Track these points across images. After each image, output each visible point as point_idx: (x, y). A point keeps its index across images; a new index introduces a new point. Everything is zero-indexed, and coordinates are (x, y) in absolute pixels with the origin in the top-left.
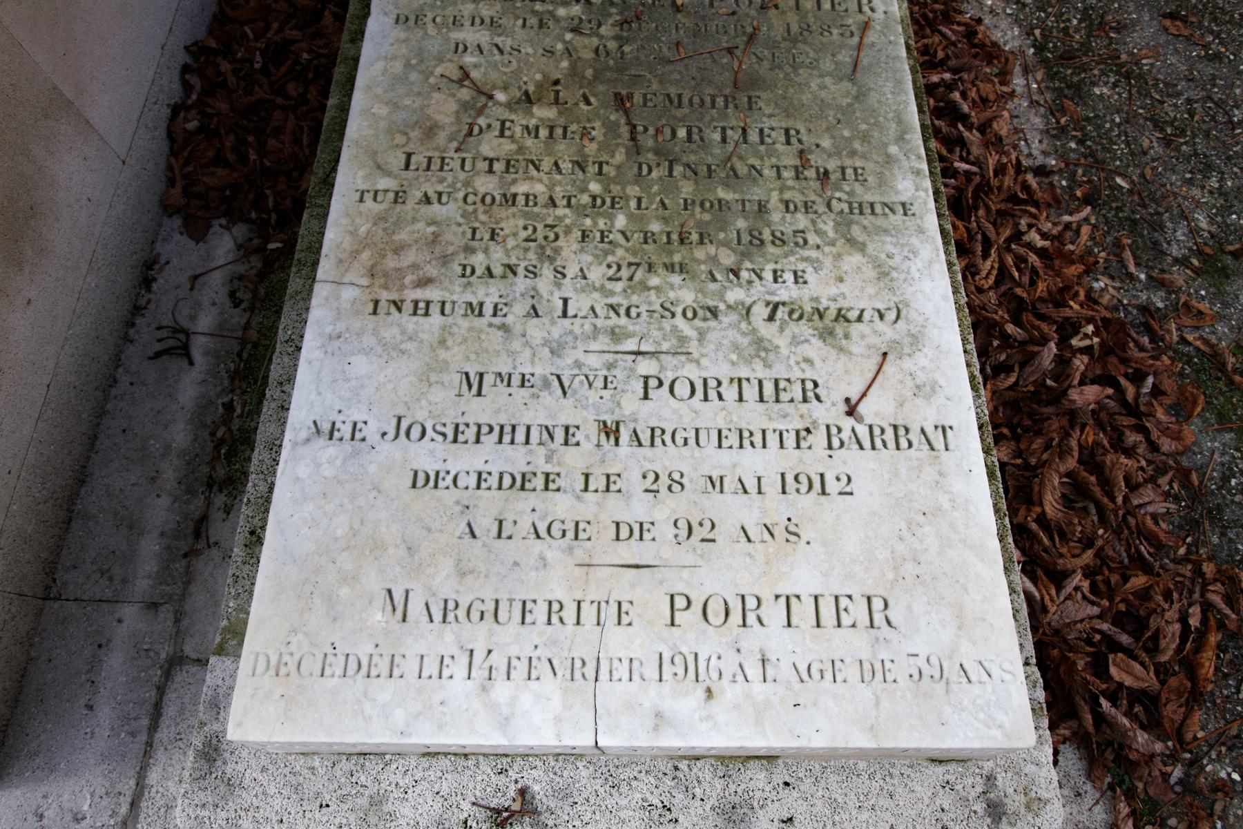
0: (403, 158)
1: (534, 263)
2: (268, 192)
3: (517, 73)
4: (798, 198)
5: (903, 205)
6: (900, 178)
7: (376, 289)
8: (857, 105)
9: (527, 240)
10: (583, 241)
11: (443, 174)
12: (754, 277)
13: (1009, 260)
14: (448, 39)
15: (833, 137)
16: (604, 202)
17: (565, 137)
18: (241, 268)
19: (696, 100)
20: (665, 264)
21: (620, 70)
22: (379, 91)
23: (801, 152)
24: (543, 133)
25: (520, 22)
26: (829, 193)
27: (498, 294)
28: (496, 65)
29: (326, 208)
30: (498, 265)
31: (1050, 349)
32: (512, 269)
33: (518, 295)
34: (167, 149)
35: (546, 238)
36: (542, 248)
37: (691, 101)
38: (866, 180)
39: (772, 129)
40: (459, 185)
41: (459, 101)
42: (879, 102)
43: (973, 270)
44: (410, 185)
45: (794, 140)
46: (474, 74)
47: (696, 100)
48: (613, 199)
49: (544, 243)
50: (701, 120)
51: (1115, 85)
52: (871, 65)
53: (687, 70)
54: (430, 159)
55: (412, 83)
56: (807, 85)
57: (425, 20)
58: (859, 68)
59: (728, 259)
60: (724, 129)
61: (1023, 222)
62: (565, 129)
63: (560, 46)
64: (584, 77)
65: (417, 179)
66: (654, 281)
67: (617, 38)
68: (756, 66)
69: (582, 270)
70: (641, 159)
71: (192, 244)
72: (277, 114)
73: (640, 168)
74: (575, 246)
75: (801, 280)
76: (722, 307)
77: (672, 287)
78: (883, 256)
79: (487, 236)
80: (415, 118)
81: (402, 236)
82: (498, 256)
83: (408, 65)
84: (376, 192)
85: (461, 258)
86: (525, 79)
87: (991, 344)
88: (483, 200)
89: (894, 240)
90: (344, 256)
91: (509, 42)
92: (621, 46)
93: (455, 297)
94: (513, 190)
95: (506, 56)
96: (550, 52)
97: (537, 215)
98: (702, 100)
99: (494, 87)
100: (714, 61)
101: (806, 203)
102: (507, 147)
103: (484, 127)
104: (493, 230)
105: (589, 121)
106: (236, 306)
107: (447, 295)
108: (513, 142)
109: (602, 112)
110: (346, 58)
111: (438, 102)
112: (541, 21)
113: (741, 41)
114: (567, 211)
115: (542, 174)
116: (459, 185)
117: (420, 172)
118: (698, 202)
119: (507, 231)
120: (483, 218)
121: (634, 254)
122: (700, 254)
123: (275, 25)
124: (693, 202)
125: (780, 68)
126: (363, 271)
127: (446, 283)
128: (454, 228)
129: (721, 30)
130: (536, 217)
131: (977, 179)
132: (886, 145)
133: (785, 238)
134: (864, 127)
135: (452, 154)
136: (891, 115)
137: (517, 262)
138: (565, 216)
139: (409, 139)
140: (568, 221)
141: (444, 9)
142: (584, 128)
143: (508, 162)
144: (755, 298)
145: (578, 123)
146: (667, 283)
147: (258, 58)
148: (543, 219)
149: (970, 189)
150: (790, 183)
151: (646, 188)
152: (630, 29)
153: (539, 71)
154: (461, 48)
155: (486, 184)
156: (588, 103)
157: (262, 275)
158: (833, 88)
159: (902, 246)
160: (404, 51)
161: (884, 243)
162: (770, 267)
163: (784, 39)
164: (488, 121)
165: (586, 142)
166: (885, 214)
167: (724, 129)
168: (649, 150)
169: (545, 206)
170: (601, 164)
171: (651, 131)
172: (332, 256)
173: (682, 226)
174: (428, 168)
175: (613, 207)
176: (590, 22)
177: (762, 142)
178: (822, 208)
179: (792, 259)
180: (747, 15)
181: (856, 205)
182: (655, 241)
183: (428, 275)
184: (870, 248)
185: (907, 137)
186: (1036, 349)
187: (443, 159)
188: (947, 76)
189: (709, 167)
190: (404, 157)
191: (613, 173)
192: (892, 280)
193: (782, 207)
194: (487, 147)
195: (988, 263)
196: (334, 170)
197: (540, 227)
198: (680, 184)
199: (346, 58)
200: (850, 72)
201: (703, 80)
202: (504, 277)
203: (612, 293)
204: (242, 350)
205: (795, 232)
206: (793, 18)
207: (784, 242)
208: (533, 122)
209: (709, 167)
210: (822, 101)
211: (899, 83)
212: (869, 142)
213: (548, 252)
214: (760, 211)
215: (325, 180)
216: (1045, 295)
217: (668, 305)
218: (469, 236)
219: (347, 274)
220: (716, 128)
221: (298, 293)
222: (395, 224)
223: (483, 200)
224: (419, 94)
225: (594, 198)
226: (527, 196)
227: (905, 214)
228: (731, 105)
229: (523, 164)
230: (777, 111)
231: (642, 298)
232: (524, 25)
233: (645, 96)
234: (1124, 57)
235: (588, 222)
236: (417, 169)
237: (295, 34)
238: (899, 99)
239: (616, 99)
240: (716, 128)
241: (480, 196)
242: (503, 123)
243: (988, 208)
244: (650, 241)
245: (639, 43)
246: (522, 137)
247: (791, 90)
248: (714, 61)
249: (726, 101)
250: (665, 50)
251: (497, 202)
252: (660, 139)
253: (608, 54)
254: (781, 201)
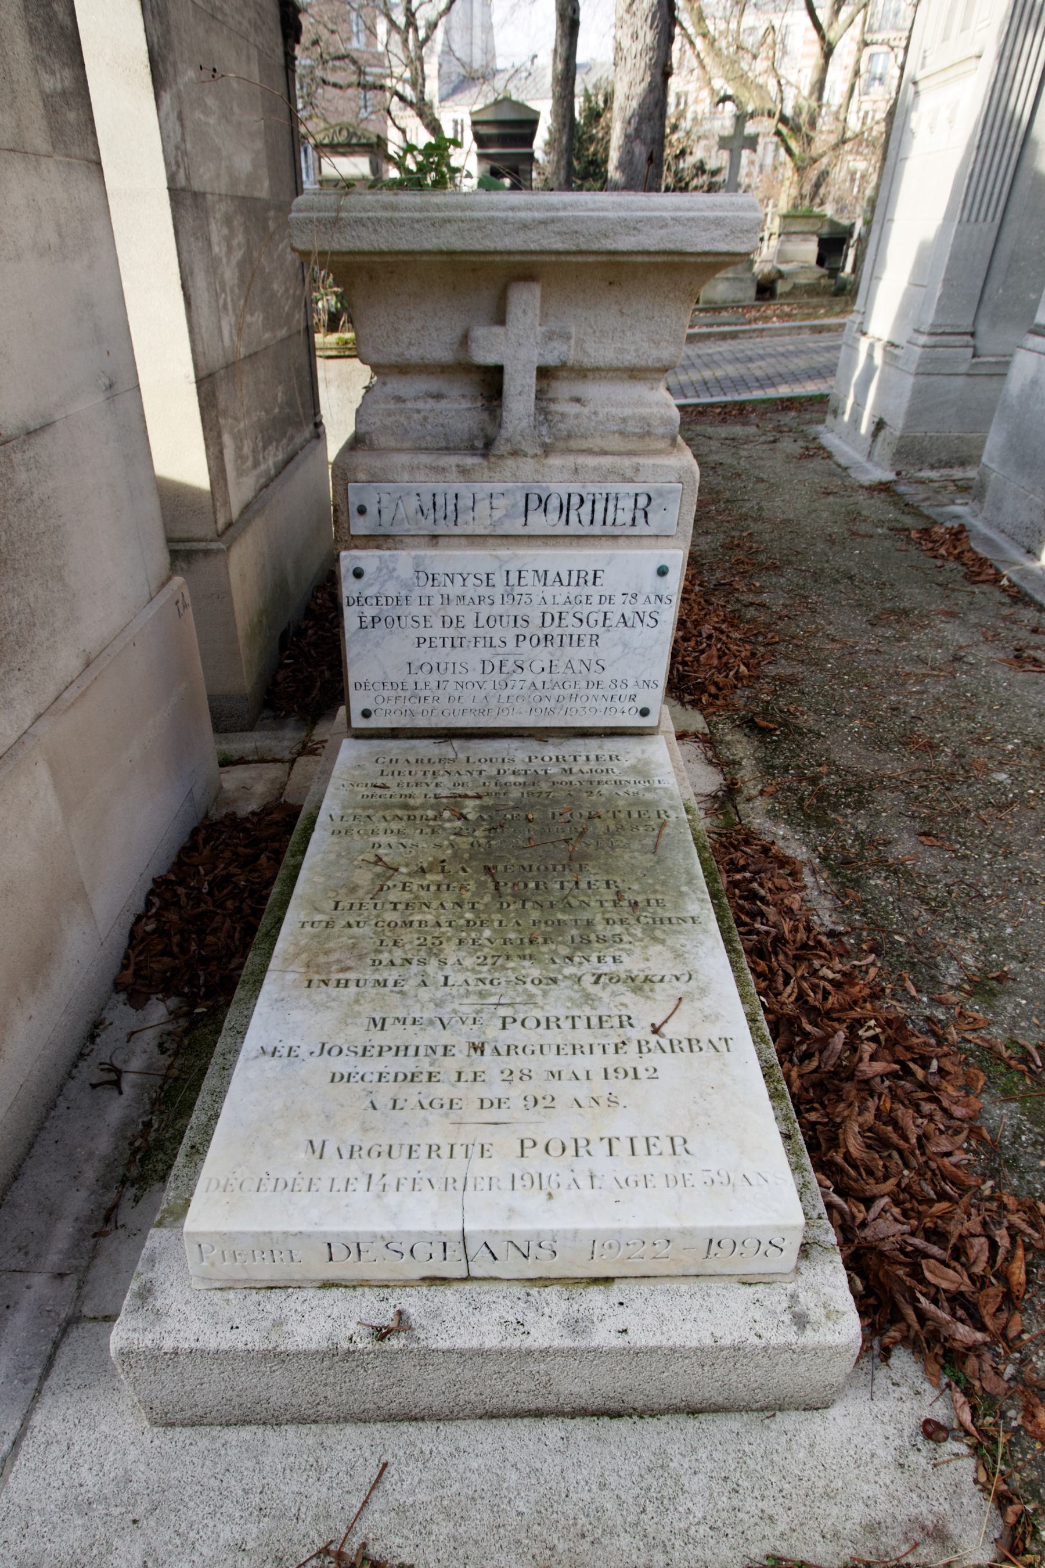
2: (201, 973)
3: (416, 857)
4: (616, 917)
18: (170, 1027)
19: (542, 868)
24: (433, 888)
34: (126, 944)
45: (613, 886)
46: (385, 859)
47: (542, 868)
51: (886, 878)
59: (564, 951)
63: (446, 843)
66: (511, 964)
67: (486, 837)
71: (133, 1011)
72: (218, 919)
76: (560, 977)
81: (331, 945)
83: (339, 855)
102: (407, 896)
106: (163, 1053)
120: (389, 934)
121: (497, 950)
122: (544, 949)
123: (222, 866)
143: (407, 905)
147: (206, 885)
155: (390, 916)
157: (186, 1032)
178: (633, 922)
184: (669, 942)
188: (748, 875)
197: (429, 938)
203: (480, 972)
234: (891, 861)
235: (464, 934)
237: (238, 871)
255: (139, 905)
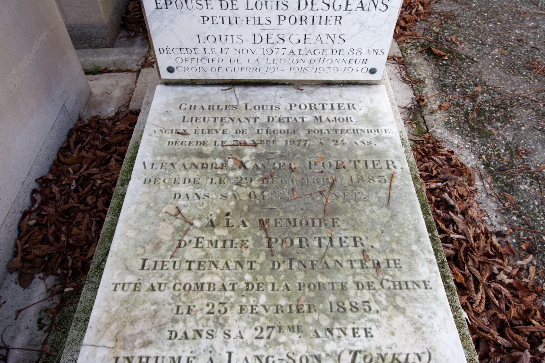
0: (141, 262)
1: (212, 328)
2: (69, 258)
3: (207, 209)
4: (364, 280)
5: (424, 282)
6: (420, 265)
7: (118, 350)
8: (392, 222)
9: (209, 313)
10: (241, 313)
11: (163, 271)
12: (341, 334)
13: (491, 294)
14: (171, 192)
15: (380, 241)
16: (253, 287)
17: (232, 247)
18: (47, 304)
19: (304, 222)
20: (289, 327)
21: (262, 206)
22: (131, 222)
23: (364, 251)
24: (220, 244)
25: (210, 180)
26: (381, 277)
27: (190, 351)
28: (196, 205)
29: (97, 285)
30: (191, 330)
31: (526, 356)
32: (199, 333)
33: (202, 351)
34: (16, 236)
35: (219, 311)
36: (217, 318)
37: (301, 222)
38: (401, 267)
39: (346, 238)
40: (171, 279)
41: (174, 227)
42: (404, 219)
43: (471, 301)
44: (144, 279)
45: (359, 244)
46: (183, 211)
47: (304, 222)
48: (258, 284)
49: (218, 315)
50: (307, 233)
51: (531, 184)
52: (397, 198)
53: (299, 204)
54: (156, 262)
55: (150, 217)
56: (364, 211)
57: (159, 181)
58: (391, 200)
59: (325, 322)
60: (320, 238)
61: (495, 268)
62: (232, 241)
63: (230, 193)
64: (243, 211)
65: (148, 275)
66: (283, 338)
67: (261, 187)
68: (336, 201)
69: (240, 332)
70: (274, 259)
71: (22, 289)
72: (80, 215)
73: (274, 264)
74: (237, 316)
75: (369, 335)
76: (323, 355)
77: (293, 342)
78: (416, 317)
79: (186, 311)
80: (149, 238)
81: (137, 313)
82: (191, 325)
83: (148, 206)
84: (124, 284)
85: (169, 327)
86: (211, 213)
87: (490, 351)
88: (184, 288)
89: (421, 305)
90: (100, 327)
91: (203, 192)
92: (263, 192)
93: (164, 354)
94: (202, 281)
95: (201, 200)
96: (225, 197)
97: (215, 296)
98: (307, 222)
99: (194, 218)
100: (313, 199)
101: (368, 283)
102: (199, 254)
103: (187, 242)
104: (189, 307)
105: (245, 236)
106: (41, 329)
107: (160, 352)
108: (203, 250)
109: (252, 230)
110: (118, 195)
111: (163, 228)
112: (221, 179)
113: (327, 187)
114: (232, 293)
115: (218, 270)
116: (171, 279)
117: (150, 271)
118: (307, 285)
119: (197, 308)
120: (184, 299)
121: (271, 320)
122: (309, 319)
123: (85, 166)
124: (304, 285)
125: (349, 201)
126: (111, 337)
127: (160, 344)
128: (167, 306)
129: (316, 181)
130: (214, 297)
131: (465, 245)
132: (410, 245)
133: (358, 306)
134: (397, 234)
135: (168, 259)
136: (411, 227)
137: (202, 328)
138: (231, 296)
139: (145, 250)
140: (232, 300)
141: (170, 174)
142: (243, 241)
143: (200, 263)
144: (343, 348)
145: (239, 238)
146: (290, 339)
147: (74, 183)
148: (218, 299)
149: (462, 250)
150: (359, 271)
151: (277, 277)
152: (268, 182)
153: (218, 208)
154: (177, 196)
155: (187, 278)
156: (245, 226)
157: (59, 308)
158: (378, 212)
159: (427, 309)
160: (147, 199)
161: (415, 307)
162: (350, 326)
163: (350, 185)
164: (190, 238)
165: (243, 249)
166: (414, 289)
167: (320, 238)
168: (278, 253)
169: (219, 290)
170: (251, 262)
171: (280, 241)
172: (94, 328)
173: (298, 301)
174: (155, 269)
175: (258, 290)
176: (246, 179)
177: (341, 246)
178: (378, 286)
179: (363, 320)
180: (329, 172)
181: (397, 283)
182: (282, 311)
183: (149, 338)
184: (408, 312)
185: (422, 239)
186: (518, 353)
187: (163, 262)
189: (312, 262)
190: (142, 261)
191: (258, 268)
192: (423, 333)
193: (355, 286)
194: (188, 254)
195: (479, 295)
196: (104, 260)
197: (216, 304)
198: (296, 274)
199: (118, 195)
200: (386, 202)
201: (307, 210)
202: (194, 338)
203: (257, 348)
204: (39, 359)
205: (364, 302)
206: (353, 173)
207: (357, 309)
208: (214, 238)
209: (312, 262)
210: (373, 220)
211: (413, 207)
212: (401, 244)
213: (221, 321)
214: (343, 289)
215: (98, 266)
216: (516, 315)
217: (291, 355)
218: (175, 311)
219: (102, 340)
220: (315, 238)
221: (73, 340)
222: (133, 305)
223: (184, 288)
224: (153, 223)
225: (248, 284)
226: (210, 284)
227: (426, 288)
228: (323, 224)
229: (208, 264)
230: (348, 227)
231: (276, 351)
232: (211, 182)
233: (276, 220)
234: (533, 169)
235: (244, 300)
236: (148, 269)
237: (95, 170)
238: (414, 217)
239: (260, 223)
240: (315, 238)
241: (183, 285)
242: (198, 239)
243: (474, 261)
244: (280, 311)
245: (272, 190)
246: (208, 247)
247: (355, 214)
248: (313, 199)
249: (320, 222)
250: (286, 193)
251: (193, 289)
252: (284, 246)
253: (256, 197)
254: (354, 282)
255: (25, 202)
